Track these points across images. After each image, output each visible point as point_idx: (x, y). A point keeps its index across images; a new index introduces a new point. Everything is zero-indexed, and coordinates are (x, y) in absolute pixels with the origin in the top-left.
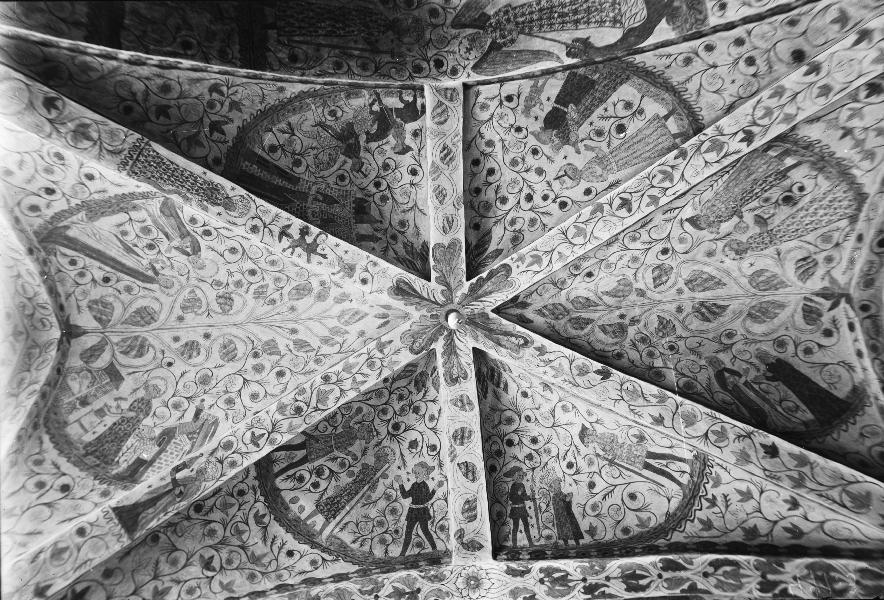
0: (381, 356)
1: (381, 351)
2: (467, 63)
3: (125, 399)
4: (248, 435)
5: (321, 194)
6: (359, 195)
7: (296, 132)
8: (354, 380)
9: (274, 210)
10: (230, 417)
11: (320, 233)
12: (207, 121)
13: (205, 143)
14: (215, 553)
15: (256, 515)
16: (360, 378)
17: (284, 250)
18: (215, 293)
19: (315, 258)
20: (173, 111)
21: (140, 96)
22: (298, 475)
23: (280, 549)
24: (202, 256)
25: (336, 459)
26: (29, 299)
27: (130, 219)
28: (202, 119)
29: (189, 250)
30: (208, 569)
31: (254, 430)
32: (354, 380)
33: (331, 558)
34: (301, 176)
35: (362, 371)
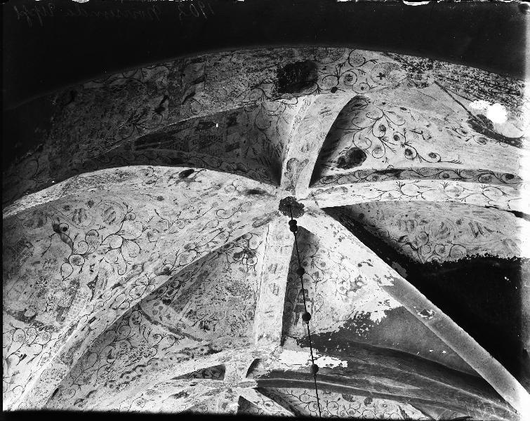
0: (229, 230)
1: (230, 228)
2: (375, 85)
3: (39, 262)
9: (166, 169)
10: (116, 271)
14: (111, 347)
33: (180, 337)
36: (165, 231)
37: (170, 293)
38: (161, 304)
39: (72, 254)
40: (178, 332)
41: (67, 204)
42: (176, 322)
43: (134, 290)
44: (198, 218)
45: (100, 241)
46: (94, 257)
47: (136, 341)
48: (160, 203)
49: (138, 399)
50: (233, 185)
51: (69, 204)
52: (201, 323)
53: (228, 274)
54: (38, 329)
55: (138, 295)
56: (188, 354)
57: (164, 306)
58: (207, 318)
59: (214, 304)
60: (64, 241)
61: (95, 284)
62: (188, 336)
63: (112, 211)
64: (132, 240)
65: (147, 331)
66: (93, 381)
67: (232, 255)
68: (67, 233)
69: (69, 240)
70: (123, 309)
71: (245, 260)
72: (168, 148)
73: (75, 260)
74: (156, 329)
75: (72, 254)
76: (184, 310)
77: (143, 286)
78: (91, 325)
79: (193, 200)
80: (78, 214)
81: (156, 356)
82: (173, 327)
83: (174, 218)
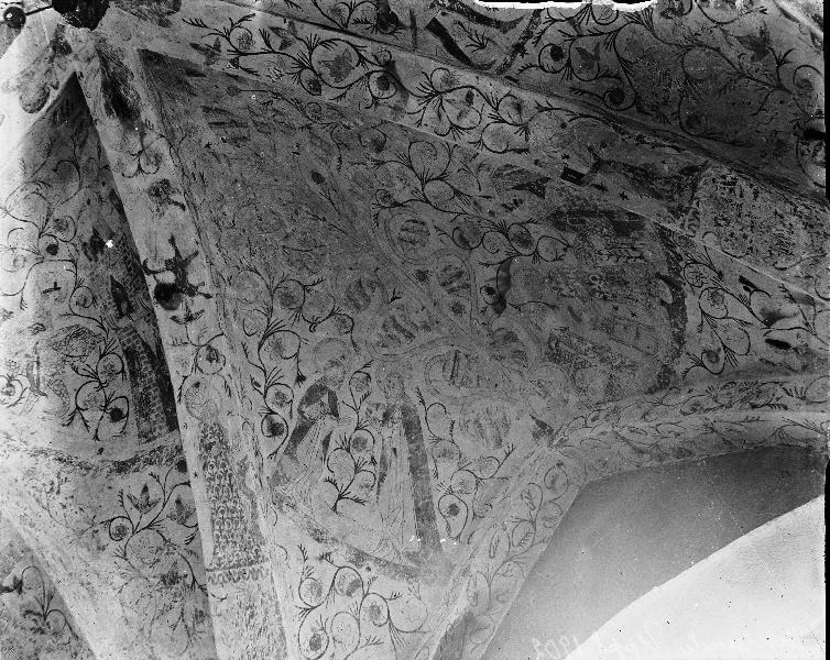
1: (217, 47)
3: (570, 309)
4: (465, 123)
5: (119, 309)
6: (82, 259)
7: (73, 408)
8: (285, 44)
12: (146, 520)
13: (173, 498)
16: (276, 42)
17: (208, 296)
18: (359, 317)
19: (185, 252)
20: (164, 568)
21: (173, 616)
24: (318, 377)
26: (533, 522)
27: (340, 497)
28: (148, 527)
29: (325, 399)
31: (455, 122)
32: (285, 44)
34: (121, 353)
35: (264, 46)
39: (519, 254)
41: (451, 315)
43: (465, 123)
46: (491, 213)
48: (323, 171)
50: (140, 168)
51: (446, 309)
54: (682, 264)
55: (469, 98)
63: (403, 233)
64: (412, 168)
68: (492, 285)
75: (519, 254)
77: (446, 105)
78: (585, 170)
79: (266, 129)
80: (455, 285)
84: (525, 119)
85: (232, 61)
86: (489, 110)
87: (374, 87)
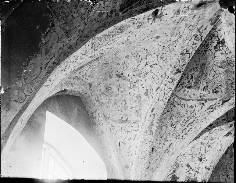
0: (199, 33)
1: (199, 32)
3: (118, 94)
9: (142, 15)
10: (154, 82)
11: (162, 8)
14: (172, 120)
15: (176, 103)
22: (182, 83)
23: (188, 107)
25: (191, 70)
30: (173, 126)
31: (167, 85)
32: (193, 48)
33: (205, 102)
36: (168, 52)
37: (189, 82)
38: (187, 90)
39: (131, 84)
40: (202, 100)
42: (199, 95)
43: (166, 87)
44: (181, 36)
45: (140, 72)
47: (182, 111)
48: (159, 40)
49: (208, 144)
50: (185, 7)
51: (118, 62)
52: (213, 91)
53: (216, 59)
54: (131, 124)
55: (170, 89)
56: (212, 108)
57: (189, 90)
58: (215, 87)
59: (216, 78)
60: (124, 79)
61: (147, 92)
62: (209, 100)
63: (139, 55)
65: (186, 106)
66: (169, 139)
67: (213, 49)
68: (124, 75)
69: (126, 78)
70: (166, 99)
71: (221, 48)
72: (139, 6)
73: (134, 86)
74: (191, 103)
75: (131, 84)
76: (200, 88)
79: (174, 29)
80: (124, 65)
81: (196, 116)
82: (199, 99)
83: (170, 43)
84: (164, 100)
85: (195, 35)
86: (167, 92)
87: (178, 67)
